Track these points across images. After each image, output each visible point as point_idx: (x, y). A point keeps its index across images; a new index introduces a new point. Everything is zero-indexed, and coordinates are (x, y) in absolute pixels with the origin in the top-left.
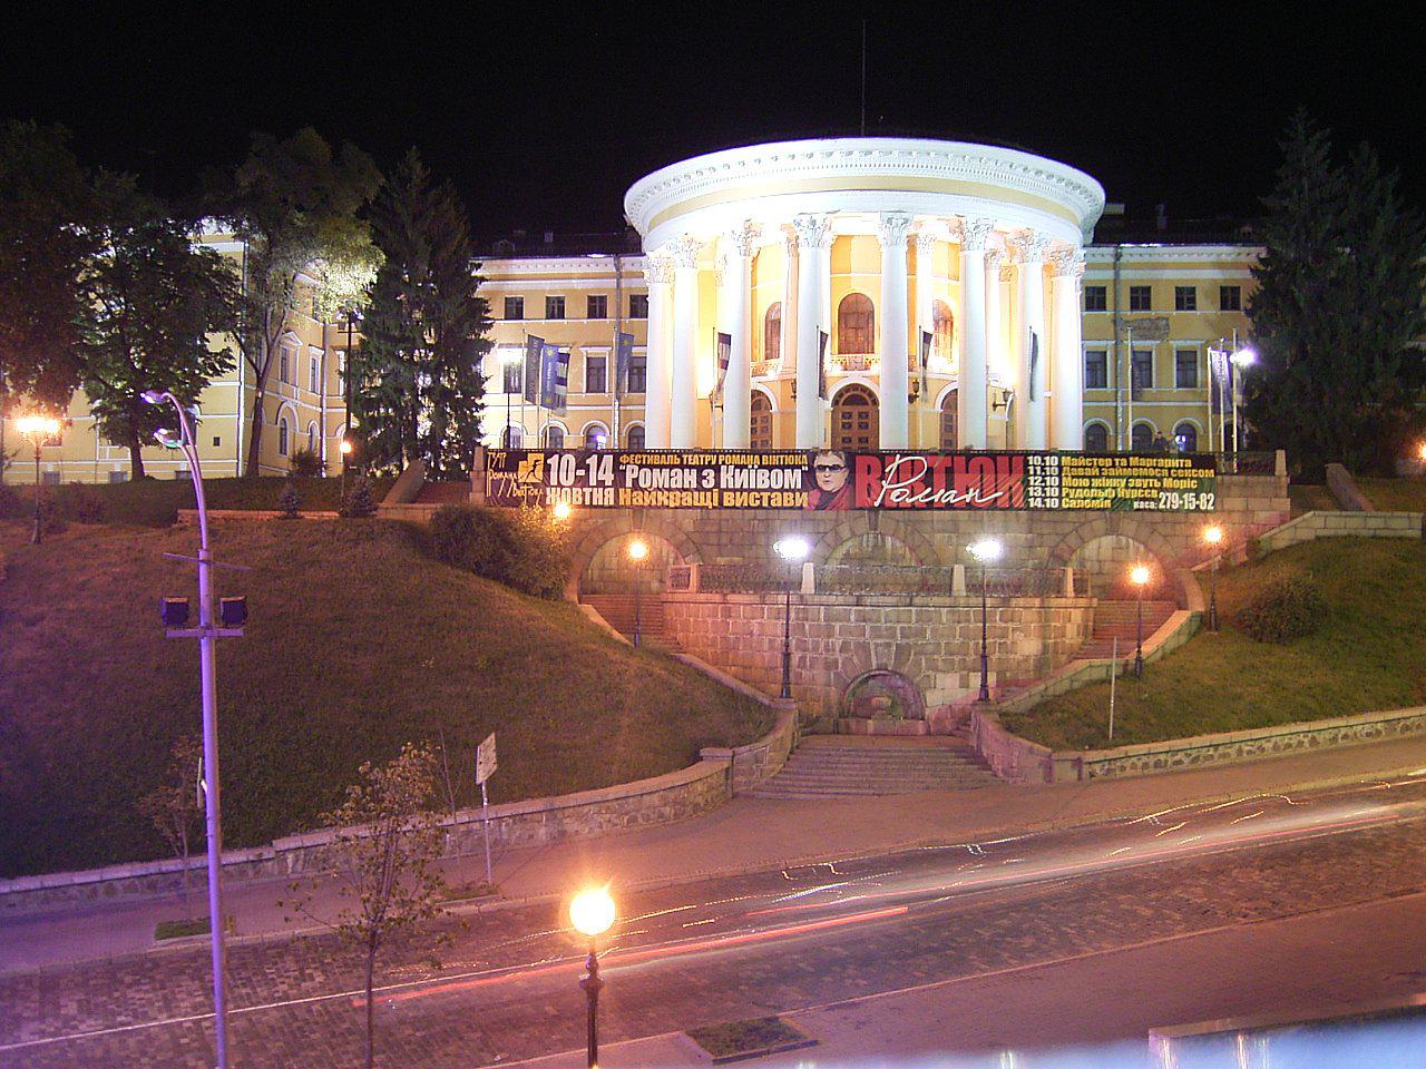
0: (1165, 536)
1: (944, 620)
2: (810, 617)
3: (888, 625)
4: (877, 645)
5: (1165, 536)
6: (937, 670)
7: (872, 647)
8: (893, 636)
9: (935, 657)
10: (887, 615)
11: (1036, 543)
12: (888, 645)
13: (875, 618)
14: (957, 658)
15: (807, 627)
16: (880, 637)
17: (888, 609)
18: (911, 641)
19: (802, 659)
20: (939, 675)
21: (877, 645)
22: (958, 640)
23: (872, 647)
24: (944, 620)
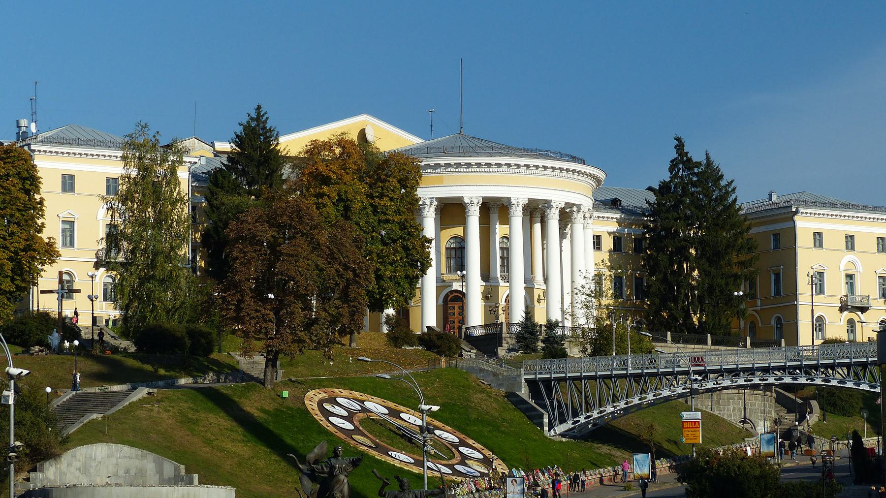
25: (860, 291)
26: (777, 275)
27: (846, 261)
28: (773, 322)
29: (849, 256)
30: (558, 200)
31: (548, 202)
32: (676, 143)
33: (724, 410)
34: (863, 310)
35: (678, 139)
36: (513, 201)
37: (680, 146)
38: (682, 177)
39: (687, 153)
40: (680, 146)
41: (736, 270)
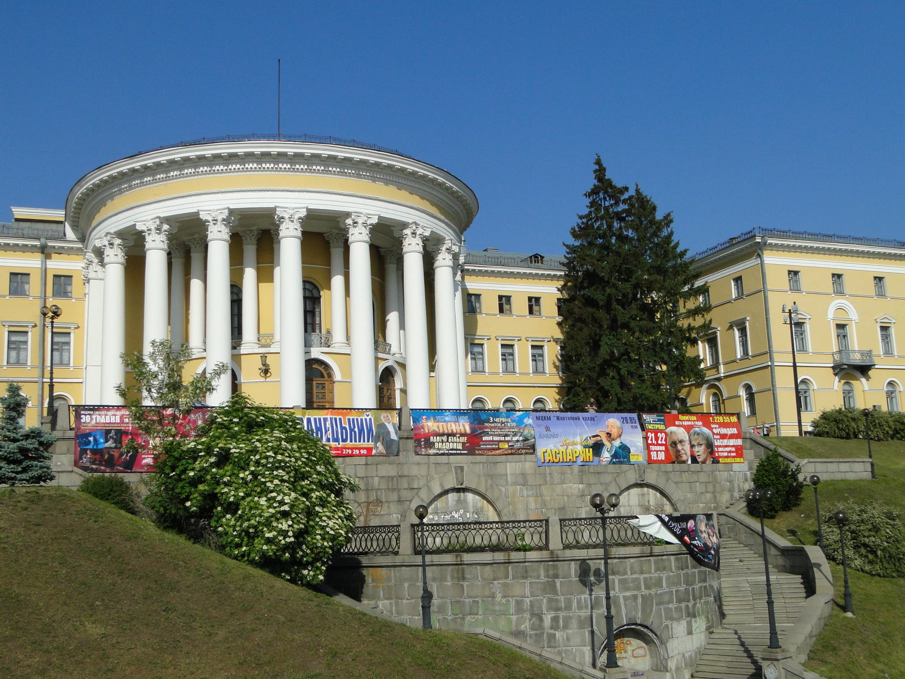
0: (676, 483)
1: (673, 568)
2: (560, 572)
3: (634, 576)
4: (625, 598)
5: (676, 483)
6: (672, 619)
7: (622, 600)
8: (638, 588)
9: (671, 606)
10: (632, 568)
11: (586, 493)
12: (635, 597)
13: (621, 569)
14: (683, 605)
15: (558, 585)
16: (628, 589)
17: (632, 560)
18: (653, 591)
19: (555, 619)
20: (675, 624)
21: (625, 598)
22: (682, 588)
23: (622, 600)
24: (673, 568)
25: (856, 343)
26: (743, 331)
27: (833, 308)
28: (742, 393)
29: (839, 301)
30: (364, 212)
31: (348, 215)
32: (597, 167)
33: (568, 607)
34: (864, 370)
35: (598, 162)
36: (279, 212)
37: (600, 172)
38: (606, 209)
39: (609, 180)
40: (600, 172)
41: (684, 323)
